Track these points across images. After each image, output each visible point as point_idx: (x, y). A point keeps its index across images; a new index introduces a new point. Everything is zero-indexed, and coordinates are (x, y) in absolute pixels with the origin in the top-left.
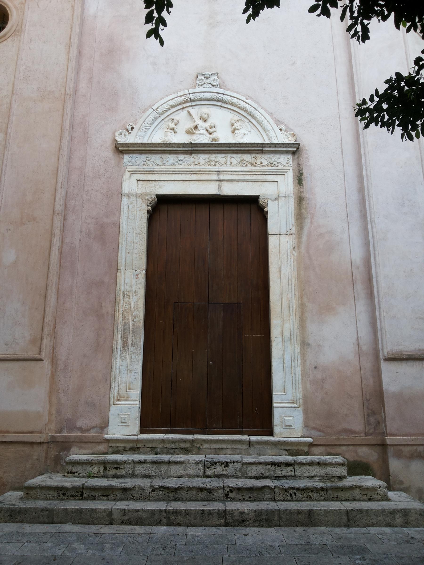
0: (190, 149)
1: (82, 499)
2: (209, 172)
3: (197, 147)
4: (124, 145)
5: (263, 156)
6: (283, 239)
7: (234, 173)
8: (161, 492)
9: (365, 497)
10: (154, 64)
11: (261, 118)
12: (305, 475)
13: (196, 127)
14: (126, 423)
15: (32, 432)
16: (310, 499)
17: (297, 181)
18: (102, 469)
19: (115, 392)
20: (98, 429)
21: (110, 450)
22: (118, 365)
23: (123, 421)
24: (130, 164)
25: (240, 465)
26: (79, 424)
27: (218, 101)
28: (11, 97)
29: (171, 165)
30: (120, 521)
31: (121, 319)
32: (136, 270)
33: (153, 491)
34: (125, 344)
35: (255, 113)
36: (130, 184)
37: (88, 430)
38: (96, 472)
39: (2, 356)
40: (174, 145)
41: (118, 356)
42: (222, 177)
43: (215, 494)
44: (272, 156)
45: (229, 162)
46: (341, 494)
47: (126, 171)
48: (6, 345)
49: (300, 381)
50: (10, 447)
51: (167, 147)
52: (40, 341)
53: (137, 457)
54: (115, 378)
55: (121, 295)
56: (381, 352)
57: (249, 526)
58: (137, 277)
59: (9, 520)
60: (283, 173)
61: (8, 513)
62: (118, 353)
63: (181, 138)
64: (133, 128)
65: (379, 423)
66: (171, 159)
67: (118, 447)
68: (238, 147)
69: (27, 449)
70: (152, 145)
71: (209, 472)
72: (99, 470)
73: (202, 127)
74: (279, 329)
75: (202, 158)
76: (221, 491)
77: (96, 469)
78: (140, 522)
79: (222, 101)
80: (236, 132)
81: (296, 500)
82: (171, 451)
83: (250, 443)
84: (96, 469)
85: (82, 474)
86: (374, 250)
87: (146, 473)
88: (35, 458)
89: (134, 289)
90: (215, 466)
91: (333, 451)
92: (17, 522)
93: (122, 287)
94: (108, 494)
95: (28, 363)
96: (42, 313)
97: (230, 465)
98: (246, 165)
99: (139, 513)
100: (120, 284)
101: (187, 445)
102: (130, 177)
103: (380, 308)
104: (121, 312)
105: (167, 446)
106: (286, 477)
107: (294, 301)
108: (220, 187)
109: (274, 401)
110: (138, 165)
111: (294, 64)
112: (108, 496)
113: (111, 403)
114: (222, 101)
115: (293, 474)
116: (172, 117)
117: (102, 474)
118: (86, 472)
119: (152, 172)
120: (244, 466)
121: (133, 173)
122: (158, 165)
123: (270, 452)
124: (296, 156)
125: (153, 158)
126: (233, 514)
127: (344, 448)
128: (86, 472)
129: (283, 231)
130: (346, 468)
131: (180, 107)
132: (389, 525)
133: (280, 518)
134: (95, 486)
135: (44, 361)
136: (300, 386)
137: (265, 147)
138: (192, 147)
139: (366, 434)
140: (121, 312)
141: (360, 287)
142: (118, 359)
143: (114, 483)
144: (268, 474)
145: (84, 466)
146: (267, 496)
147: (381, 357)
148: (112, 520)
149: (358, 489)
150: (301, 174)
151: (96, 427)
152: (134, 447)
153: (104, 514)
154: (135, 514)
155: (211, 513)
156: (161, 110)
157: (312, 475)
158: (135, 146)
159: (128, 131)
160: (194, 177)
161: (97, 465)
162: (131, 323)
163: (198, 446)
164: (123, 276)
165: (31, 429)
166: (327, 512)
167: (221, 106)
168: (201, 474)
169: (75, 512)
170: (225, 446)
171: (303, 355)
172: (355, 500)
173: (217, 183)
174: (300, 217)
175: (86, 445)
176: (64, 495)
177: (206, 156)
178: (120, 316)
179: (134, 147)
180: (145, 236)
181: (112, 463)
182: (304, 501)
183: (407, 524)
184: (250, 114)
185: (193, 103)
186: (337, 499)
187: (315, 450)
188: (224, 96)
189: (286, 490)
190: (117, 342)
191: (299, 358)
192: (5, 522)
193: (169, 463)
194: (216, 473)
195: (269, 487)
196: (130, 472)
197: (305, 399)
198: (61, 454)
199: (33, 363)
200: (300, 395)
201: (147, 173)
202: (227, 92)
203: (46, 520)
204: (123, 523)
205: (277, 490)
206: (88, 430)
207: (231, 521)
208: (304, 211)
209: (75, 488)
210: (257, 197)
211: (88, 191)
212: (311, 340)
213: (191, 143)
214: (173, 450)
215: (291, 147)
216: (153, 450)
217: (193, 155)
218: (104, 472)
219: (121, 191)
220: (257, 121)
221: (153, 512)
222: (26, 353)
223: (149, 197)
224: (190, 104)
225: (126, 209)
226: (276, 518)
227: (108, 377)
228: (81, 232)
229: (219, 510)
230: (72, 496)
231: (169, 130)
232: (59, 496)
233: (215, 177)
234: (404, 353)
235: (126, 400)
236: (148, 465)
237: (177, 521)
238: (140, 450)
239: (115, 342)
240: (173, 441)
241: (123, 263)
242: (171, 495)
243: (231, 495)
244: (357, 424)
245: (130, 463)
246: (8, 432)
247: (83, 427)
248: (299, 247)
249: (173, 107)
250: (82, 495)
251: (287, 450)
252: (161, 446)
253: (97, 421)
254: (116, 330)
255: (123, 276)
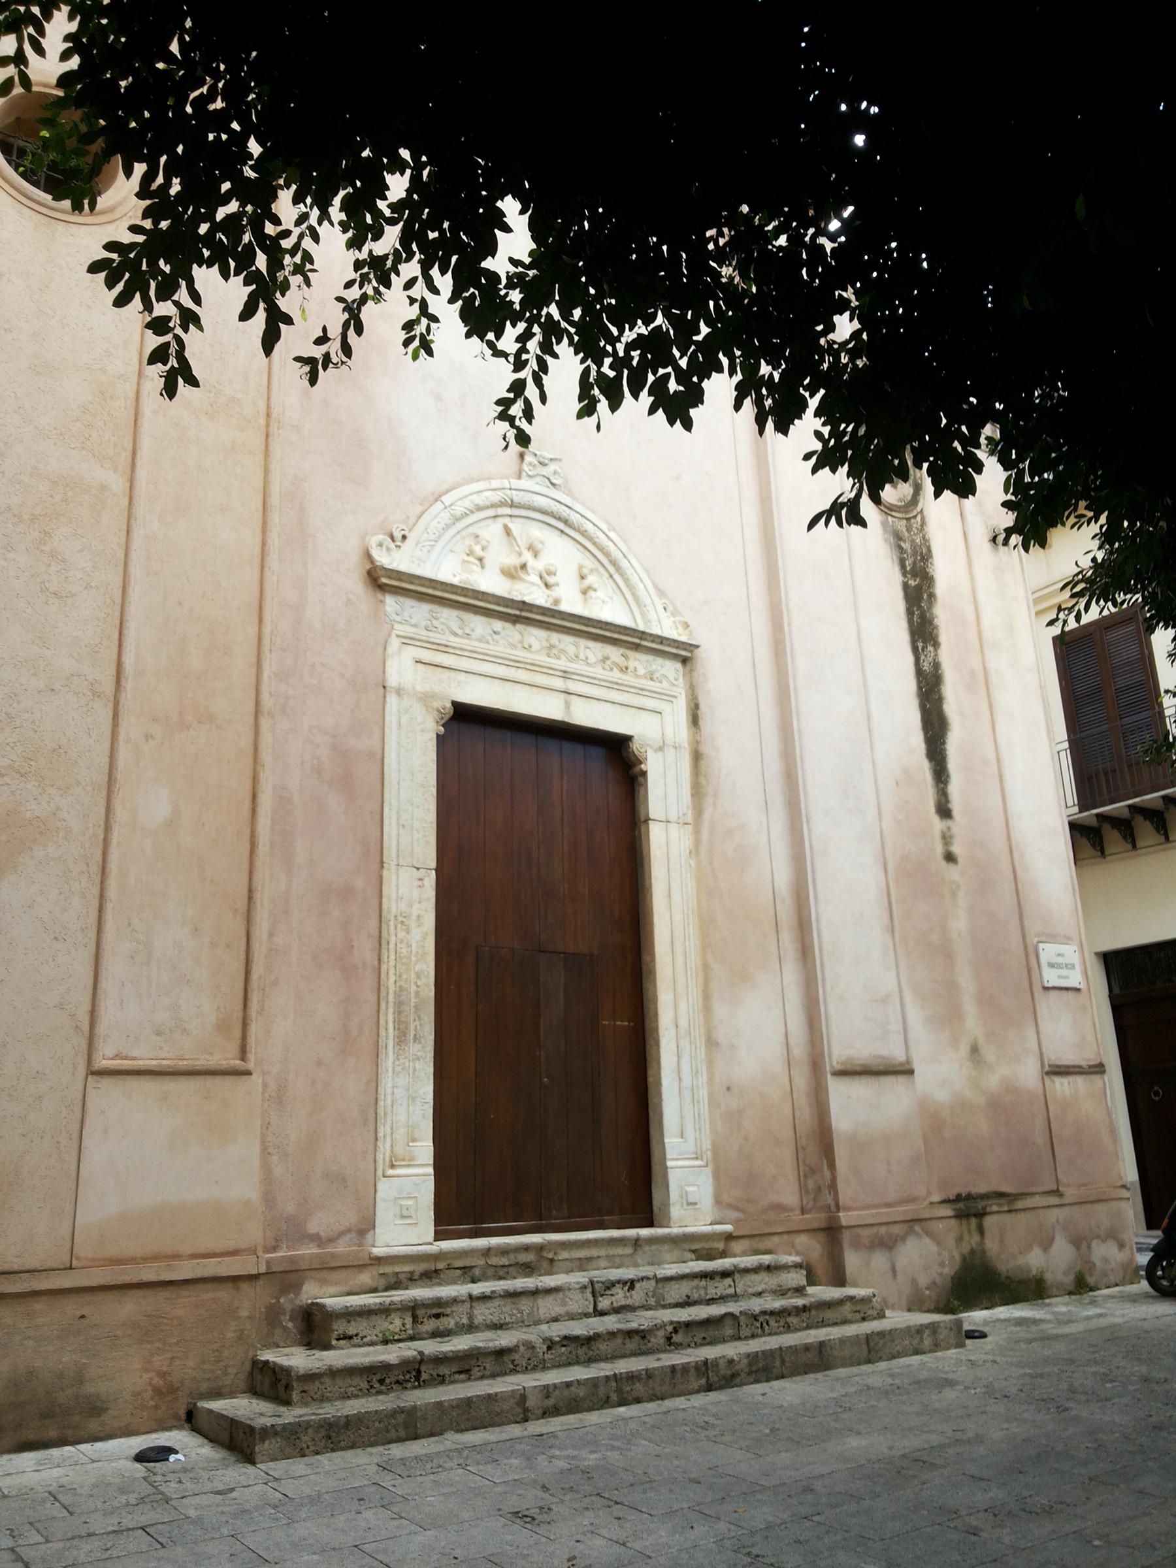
0: (518, 613)
1: (420, 1385)
2: (550, 671)
3: (531, 611)
4: (394, 575)
5: (638, 655)
6: (673, 829)
8: (563, 1349)
9: (858, 1316)
10: (438, 398)
11: (634, 579)
12: (750, 1290)
13: (524, 566)
14: (410, 1217)
15: (234, 1253)
16: (788, 1328)
17: (690, 718)
18: (409, 1321)
19: (384, 1149)
20: (353, 1235)
21: (382, 1283)
22: (390, 1085)
23: (405, 1213)
24: (398, 619)
25: (653, 1283)
26: (313, 1227)
27: (560, 519)
28: (138, 384)
29: (480, 640)
30: (540, 1412)
31: (392, 979)
32: (418, 869)
33: (549, 1348)
34: (401, 1037)
35: (624, 563)
36: (402, 668)
37: (331, 1240)
38: (397, 1330)
39: (154, 1062)
40: (490, 599)
41: (390, 1065)
42: (573, 686)
43: (652, 1340)
44: (651, 658)
45: (582, 657)
46: (829, 1315)
47: (393, 636)
48: (159, 1034)
49: (707, 1115)
50: (184, 1293)
51: (477, 598)
52: (239, 1026)
53: (477, 1289)
54: (385, 1114)
55: (392, 923)
56: (827, 1059)
57: (741, 1385)
58: (420, 883)
59: (326, 1447)
60: (670, 698)
61: (323, 1433)
62: (389, 1059)
63: (490, 582)
64: (404, 537)
65: (820, 1188)
66: (479, 625)
67: (397, 1273)
68: (601, 628)
69: (224, 1294)
70: (448, 588)
71: (604, 1304)
72: (404, 1325)
73: (533, 569)
74: (671, 1013)
75: (536, 637)
76: (661, 1333)
77: (398, 1322)
78: (574, 1406)
79: (566, 522)
80: (591, 593)
81: (770, 1334)
82: (501, 1273)
83: (637, 1242)
84: (398, 1322)
85: (369, 1338)
86: (813, 873)
87: (495, 1319)
88: (244, 1313)
89: (415, 911)
90: (613, 1291)
91: (761, 1246)
92: (342, 1449)
93: (392, 906)
94: (467, 1367)
95: (217, 1081)
96: (243, 956)
97: (637, 1285)
98: (612, 669)
99: (572, 1388)
100: (389, 899)
101: (530, 1257)
102: (400, 650)
103: (823, 979)
104: (392, 963)
105: (494, 1261)
106: (723, 1299)
107: (694, 959)
108: (568, 705)
109: (668, 1156)
110: (415, 626)
111: (678, 478)
112: (467, 1371)
113: (380, 1173)
114: (566, 522)
115: (732, 1291)
116: (474, 529)
117: (410, 1332)
118: (376, 1331)
119: (443, 648)
120: (660, 1286)
121: (407, 641)
122: (456, 634)
123: (667, 1257)
124: (688, 668)
125: (445, 615)
126: (717, 1365)
127: (776, 1239)
128: (376, 1331)
129: (673, 817)
130: (804, 1272)
131: (491, 512)
132: (917, 1352)
133: (783, 1362)
134: (445, 1353)
135: (254, 1077)
136: (707, 1126)
137: (645, 639)
138: (521, 610)
139: (803, 1212)
140: (392, 963)
141: (788, 938)
142: (390, 1070)
143: (431, 1347)
144: (695, 1296)
145: (373, 1318)
146: (729, 1331)
147: (828, 1068)
148: (526, 1410)
149: (848, 1304)
150: (697, 706)
151: (349, 1230)
152: (431, 1270)
153: (513, 1401)
154: (566, 1393)
155: (685, 1368)
156: (459, 510)
157: (760, 1290)
158: (416, 581)
159: (392, 538)
160: (522, 675)
161: (399, 1313)
162: (413, 988)
163: (550, 1256)
164: (394, 878)
165: (231, 1245)
166: (843, 1341)
167: (562, 531)
168: (591, 1310)
169: (458, 1406)
170: (595, 1252)
171: (710, 1063)
172: (845, 1322)
173: (564, 695)
174: (698, 791)
175: (335, 1276)
176: (381, 1382)
177: (542, 634)
178: (392, 971)
179: (412, 583)
180: (434, 791)
181: (379, 1310)
182: (781, 1333)
183: (936, 1347)
184: (614, 563)
185: (516, 512)
186: (822, 1324)
187: (736, 1246)
188: (572, 513)
189: (755, 1317)
190: (387, 1032)
191: (705, 1070)
192: (317, 1453)
193: (535, 1293)
194: (615, 1305)
195: (731, 1315)
196: (465, 1321)
197: (715, 1149)
198: (282, 1300)
199: (228, 1081)
200: (707, 1144)
201: (435, 647)
202: (577, 507)
203: (403, 1434)
204: (546, 1413)
205: (743, 1320)
206: (331, 1240)
207: (716, 1379)
208: (703, 781)
209: (405, 1364)
210: (627, 739)
211: (313, 665)
212: (720, 1036)
213: (524, 602)
214: (505, 1270)
215: (685, 650)
216: (468, 1274)
217: (518, 626)
218: (413, 1329)
219: (384, 680)
220: (627, 581)
221: (594, 1383)
222: (207, 1057)
223: (437, 704)
224: (508, 511)
225: (394, 725)
226: (778, 1364)
227: (370, 1114)
228: (303, 763)
229: (697, 1362)
230: (397, 1382)
231: (471, 559)
232: (372, 1387)
233: (559, 683)
234: (857, 1062)
235: (408, 1166)
236: (497, 1302)
237: (635, 1394)
238: (442, 1276)
239: (382, 1033)
240: (504, 1251)
241: (394, 851)
242: (581, 1352)
243: (676, 1338)
244: (789, 1196)
245: (463, 1301)
246: (177, 1256)
247: (322, 1234)
248: (697, 850)
249: (479, 509)
250: (417, 1378)
251: (693, 1251)
252: (482, 1262)
253: (350, 1218)
254: (383, 1005)
255: (394, 878)
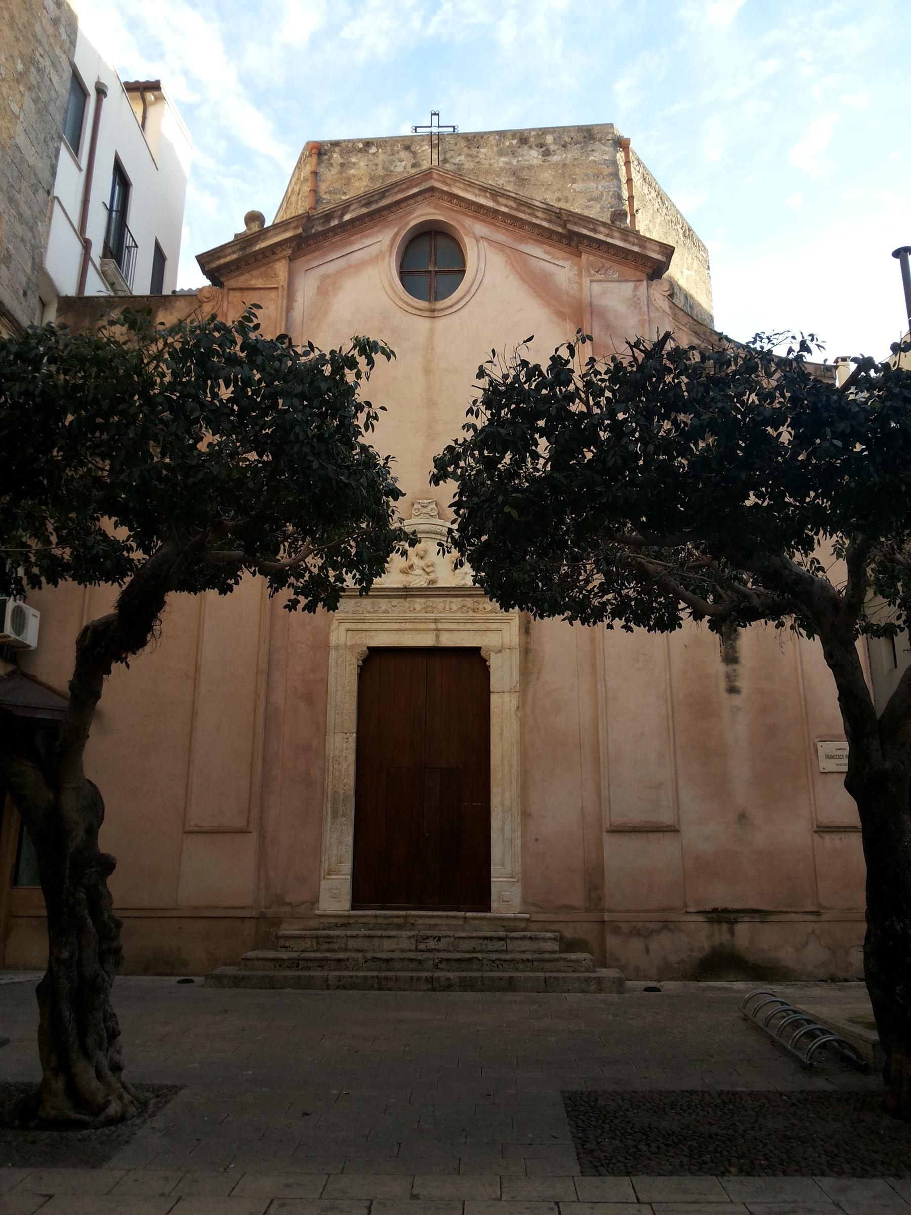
2: (425, 621)
6: (507, 697)
7: (453, 620)
13: (411, 567)
15: (242, 908)
19: (325, 866)
25: (452, 939)
26: (288, 900)
31: (330, 787)
34: (335, 815)
42: (440, 626)
45: (447, 608)
57: (454, 991)
71: (422, 946)
75: (419, 603)
93: (331, 752)
97: (442, 939)
98: (468, 612)
101: (401, 921)
108: (437, 637)
119: (363, 621)
122: (369, 612)
132: (583, 991)
133: (483, 984)
144: (479, 948)
155: (419, 979)
160: (409, 626)
168: (414, 948)
171: (524, 826)
173: (435, 632)
176: (280, 966)
177: (423, 600)
180: (356, 694)
183: (600, 990)
187: (533, 926)
189: (493, 961)
191: (520, 829)
196: (343, 946)
200: (518, 869)
210: (478, 649)
221: (365, 978)
223: (359, 650)
226: (479, 984)
227: (317, 851)
233: (432, 626)
236: (360, 940)
239: (325, 813)
241: (332, 725)
243: (440, 966)
244: (578, 901)
250: (297, 966)
